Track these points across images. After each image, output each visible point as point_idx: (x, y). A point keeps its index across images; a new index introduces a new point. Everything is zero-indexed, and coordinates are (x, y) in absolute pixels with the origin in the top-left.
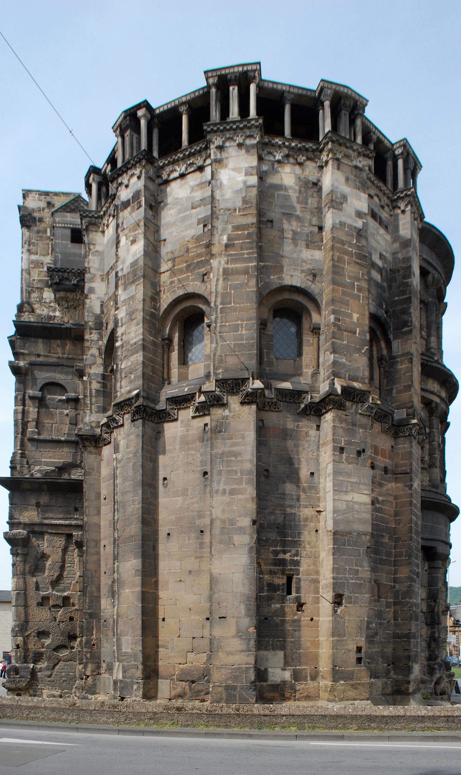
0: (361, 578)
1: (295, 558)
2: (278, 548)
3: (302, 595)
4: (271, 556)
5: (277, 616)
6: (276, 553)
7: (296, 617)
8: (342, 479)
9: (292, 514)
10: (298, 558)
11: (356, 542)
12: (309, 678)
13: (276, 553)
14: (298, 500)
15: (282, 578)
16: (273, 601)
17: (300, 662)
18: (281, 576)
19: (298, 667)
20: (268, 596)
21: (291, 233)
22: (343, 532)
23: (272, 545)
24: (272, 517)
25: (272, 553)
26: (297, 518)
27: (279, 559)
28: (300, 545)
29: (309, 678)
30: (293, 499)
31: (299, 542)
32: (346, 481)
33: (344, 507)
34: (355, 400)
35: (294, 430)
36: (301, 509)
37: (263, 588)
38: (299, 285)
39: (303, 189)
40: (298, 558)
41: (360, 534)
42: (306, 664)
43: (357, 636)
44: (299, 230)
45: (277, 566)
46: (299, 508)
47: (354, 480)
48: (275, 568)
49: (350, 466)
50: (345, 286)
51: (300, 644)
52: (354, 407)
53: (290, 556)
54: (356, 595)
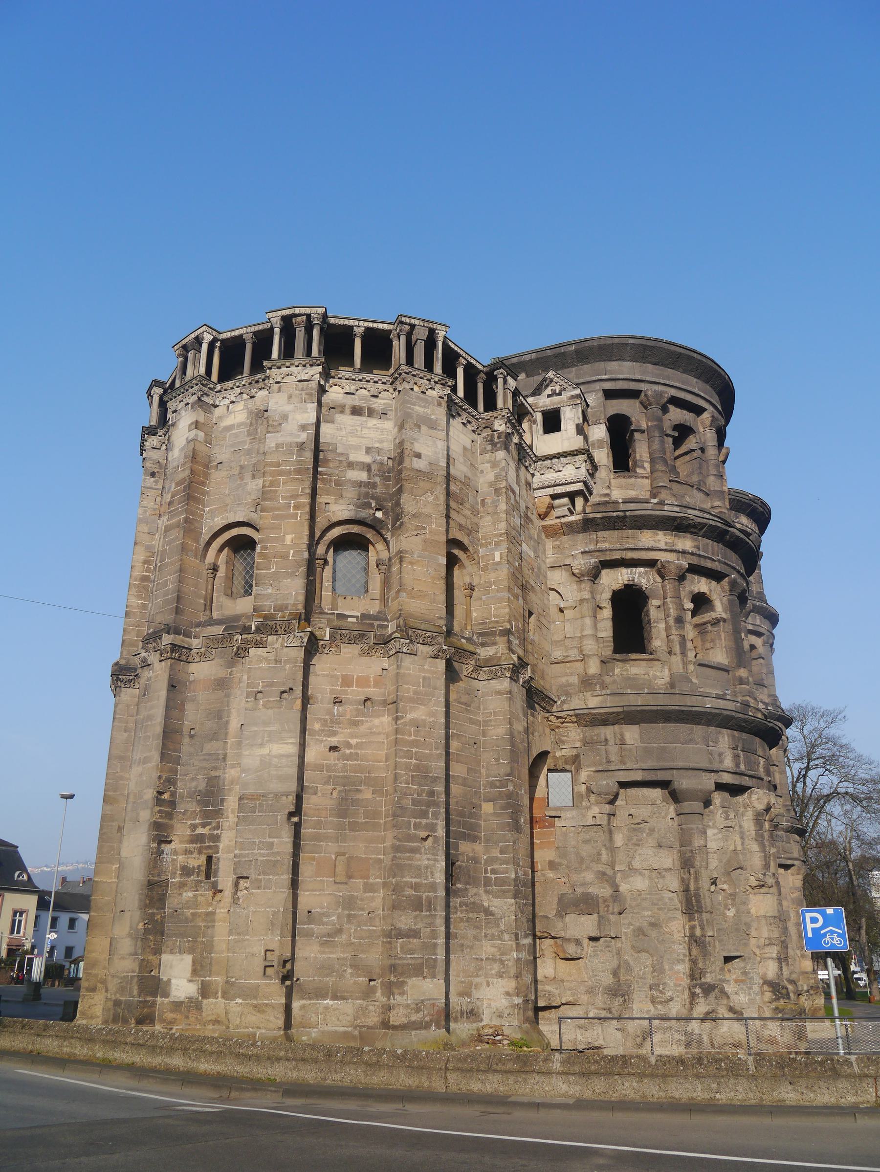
0: (277, 853)
1: (216, 832)
2: (197, 821)
3: (220, 879)
4: (188, 832)
5: (188, 908)
6: (194, 827)
7: (210, 909)
9: (216, 777)
12: (220, 994)
13: (194, 827)
14: (224, 759)
17: (210, 971)
19: (207, 978)
20: (180, 882)
21: (238, 468)
23: (190, 818)
24: (194, 784)
26: (221, 783)
27: (197, 835)
28: (222, 814)
29: (220, 994)
33: (258, 762)
38: (241, 520)
39: (254, 421)
40: (219, 832)
42: (218, 975)
43: (266, 935)
46: (224, 769)
48: (192, 846)
49: (270, 712)
52: (280, 640)
53: (210, 830)
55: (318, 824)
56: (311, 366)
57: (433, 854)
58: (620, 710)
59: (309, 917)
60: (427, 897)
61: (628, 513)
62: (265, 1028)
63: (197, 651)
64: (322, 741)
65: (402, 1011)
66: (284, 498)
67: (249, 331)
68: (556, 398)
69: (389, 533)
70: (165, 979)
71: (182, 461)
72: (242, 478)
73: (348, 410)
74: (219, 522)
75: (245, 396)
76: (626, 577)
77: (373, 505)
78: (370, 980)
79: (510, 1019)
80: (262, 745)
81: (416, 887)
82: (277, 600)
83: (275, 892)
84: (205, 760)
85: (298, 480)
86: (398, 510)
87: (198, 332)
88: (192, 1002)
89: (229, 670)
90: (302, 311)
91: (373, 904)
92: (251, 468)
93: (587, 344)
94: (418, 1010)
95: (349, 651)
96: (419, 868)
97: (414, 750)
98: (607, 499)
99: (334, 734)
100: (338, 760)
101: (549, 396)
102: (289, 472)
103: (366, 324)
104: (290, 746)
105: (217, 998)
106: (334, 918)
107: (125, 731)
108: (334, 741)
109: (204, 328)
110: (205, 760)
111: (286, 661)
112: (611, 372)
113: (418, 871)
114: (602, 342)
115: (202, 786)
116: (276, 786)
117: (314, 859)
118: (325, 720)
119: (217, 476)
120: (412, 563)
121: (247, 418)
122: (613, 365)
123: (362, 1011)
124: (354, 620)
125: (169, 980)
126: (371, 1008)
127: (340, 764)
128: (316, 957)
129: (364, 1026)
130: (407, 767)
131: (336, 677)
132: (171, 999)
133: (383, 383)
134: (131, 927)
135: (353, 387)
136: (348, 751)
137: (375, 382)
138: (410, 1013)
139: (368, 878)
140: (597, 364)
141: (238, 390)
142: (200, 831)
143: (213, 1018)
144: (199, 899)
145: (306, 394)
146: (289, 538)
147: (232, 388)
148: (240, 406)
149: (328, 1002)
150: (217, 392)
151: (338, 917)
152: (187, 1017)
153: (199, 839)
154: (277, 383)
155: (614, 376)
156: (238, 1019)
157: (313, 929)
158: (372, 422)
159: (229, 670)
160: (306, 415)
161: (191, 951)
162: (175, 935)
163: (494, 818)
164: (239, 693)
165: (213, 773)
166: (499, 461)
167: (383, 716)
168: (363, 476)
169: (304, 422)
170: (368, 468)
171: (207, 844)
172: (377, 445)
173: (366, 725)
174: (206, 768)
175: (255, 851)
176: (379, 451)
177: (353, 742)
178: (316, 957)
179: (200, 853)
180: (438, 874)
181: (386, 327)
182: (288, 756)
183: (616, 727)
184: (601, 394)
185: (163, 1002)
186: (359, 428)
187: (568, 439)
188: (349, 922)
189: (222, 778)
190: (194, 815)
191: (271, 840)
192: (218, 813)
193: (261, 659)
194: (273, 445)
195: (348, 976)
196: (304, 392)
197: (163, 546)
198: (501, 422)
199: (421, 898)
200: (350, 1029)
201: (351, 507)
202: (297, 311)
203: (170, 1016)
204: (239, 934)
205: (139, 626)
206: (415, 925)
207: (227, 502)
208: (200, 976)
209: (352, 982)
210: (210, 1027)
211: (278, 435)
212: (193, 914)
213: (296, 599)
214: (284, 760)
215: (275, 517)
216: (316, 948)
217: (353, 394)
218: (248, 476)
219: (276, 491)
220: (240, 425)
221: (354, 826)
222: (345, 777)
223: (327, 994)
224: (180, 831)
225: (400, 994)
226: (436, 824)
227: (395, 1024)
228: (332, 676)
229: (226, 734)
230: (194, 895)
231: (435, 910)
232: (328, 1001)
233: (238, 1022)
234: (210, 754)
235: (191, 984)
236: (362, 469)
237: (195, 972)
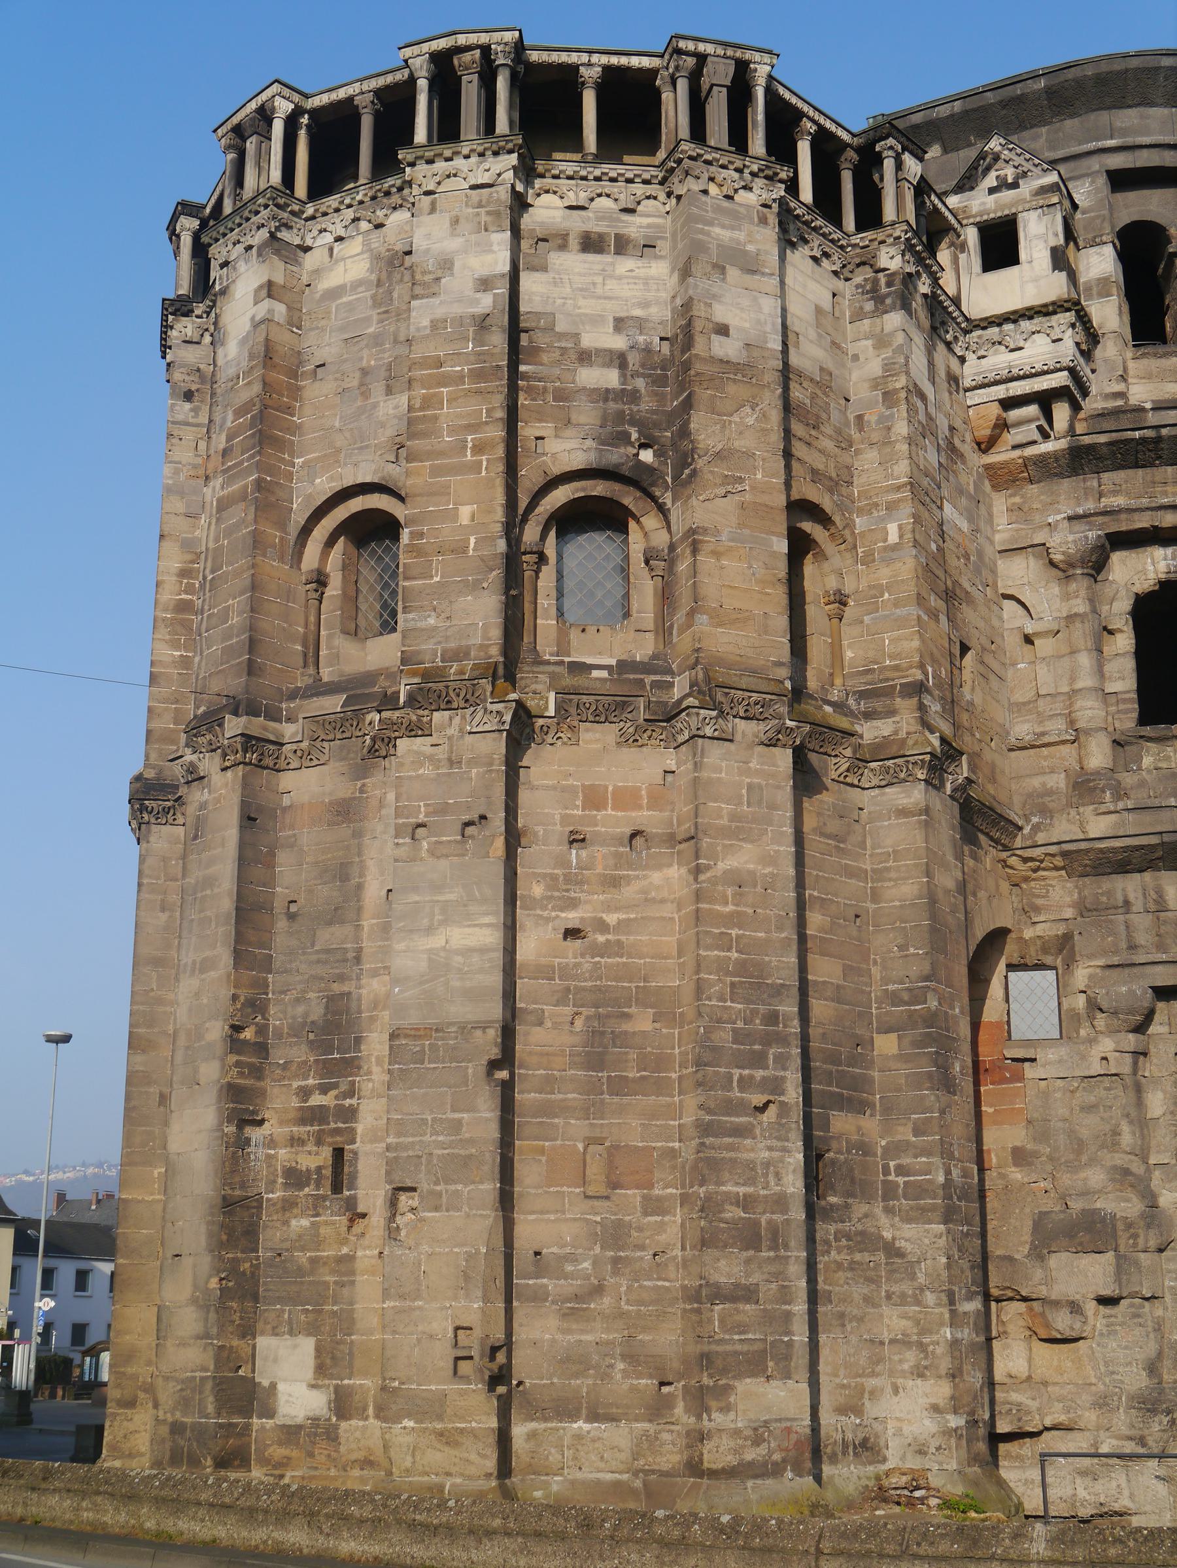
0: (471, 1142)
1: (348, 1102)
2: (311, 1082)
3: (360, 1193)
4: (295, 1103)
5: (303, 1249)
6: (305, 1093)
7: (345, 1250)
8: (417, 898)
9: (342, 995)
10: (354, 1101)
11: (454, 1048)
12: (371, 1411)
13: (305, 1093)
14: (358, 960)
15: (317, 1154)
16: (295, 1211)
17: (351, 1366)
18: (315, 1148)
19: (346, 1382)
20: (284, 1200)
21: (358, 374)
22: (418, 1029)
23: (296, 1076)
24: (300, 1009)
25: (297, 1094)
26: (354, 1005)
27: (312, 1108)
28: (359, 1068)
29: (371, 1411)
30: (346, 960)
31: (356, 1063)
32: (429, 902)
33: (424, 965)
34: (455, 705)
35: (354, 798)
36: (363, 982)
37: (275, 1182)
38: (368, 480)
39: (384, 275)
40: (354, 1101)
41: (465, 1029)
42: (365, 1374)
43: (455, 1298)
44: (373, 363)
45: (305, 1125)
46: (358, 979)
47: (451, 897)
48: (303, 1129)
49: (444, 864)
50: (441, 454)
51: (353, 1321)
52: (457, 720)
53: (337, 1097)
54: (453, 1187)
55: (549, 1084)
56: (496, 154)
57: (779, 1139)
58: (1154, 840)
59: (537, 1264)
60: (769, 1222)
61: (1164, 432)
62: (462, 1475)
63: (294, 747)
64: (548, 920)
65: (726, 1442)
66: (452, 430)
67: (365, 87)
68: (1007, 195)
69: (669, 494)
70: (266, 1383)
71: (244, 364)
72: (366, 395)
73: (574, 243)
74: (324, 486)
75: (364, 225)
76: (1162, 566)
77: (634, 436)
78: (662, 1384)
79: (940, 1458)
80: (430, 930)
81: (746, 1203)
82: (447, 638)
83: (468, 1216)
84: (318, 961)
85: (478, 392)
86: (685, 445)
87: (264, 97)
88: (318, 1426)
89: (359, 784)
90: (473, 39)
91: (663, 1238)
92: (383, 374)
93: (1070, 74)
94: (757, 1441)
95: (597, 737)
96: (750, 1166)
97: (734, 932)
98: (1120, 403)
99: (573, 904)
100: (583, 955)
101: (992, 191)
102: (460, 378)
103: (604, 60)
104: (487, 931)
105: (366, 1419)
106: (586, 1265)
107: (163, 910)
108: (572, 917)
109: (276, 88)
110: (318, 961)
111: (473, 762)
112: (1124, 132)
113: (750, 1172)
114: (1104, 67)
115: (317, 1012)
116: (460, 1011)
117: (542, 1151)
118: (554, 878)
119: (316, 392)
120: (717, 554)
121: (371, 270)
122: (1128, 118)
123: (651, 1442)
124: (604, 674)
125: (273, 1386)
126: (665, 1436)
127: (587, 964)
128: (554, 1341)
129: (653, 1472)
130: (722, 967)
131: (572, 790)
132: (279, 1420)
133: (646, 182)
134: (195, 1287)
135: (582, 195)
136: (601, 939)
137: (629, 181)
138: (743, 1447)
139: (651, 1186)
140: (1093, 116)
141: (349, 214)
142: (317, 1100)
143: (359, 1455)
144: (322, 1231)
145: (488, 213)
146: (465, 512)
147: (337, 210)
148: (355, 246)
149: (581, 1425)
150: (307, 220)
151: (594, 1264)
152: (311, 1455)
153: (316, 1116)
154: (428, 193)
155: (1129, 141)
156: (409, 1459)
157: (546, 1286)
158: (626, 265)
159: (359, 784)
160: (489, 258)
161: (312, 1329)
162: (279, 1300)
163: (899, 1065)
164: (380, 828)
165: (337, 988)
166: (892, 334)
167: (670, 865)
168: (611, 378)
169: (485, 272)
170: (619, 360)
171: (333, 1125)
172: (638, 312)
173: (636, 886)
174: (322, 978)
175: (427, 1138)
176: (641, 324)
177: (611, 919)
178: (554, 1341)
179: (319, 1142)
180: (791, 1177)
181: (645, 62)
182: (482, 950)
183: (1147, 876)
184: (1102, 180)
186: (599, 279)
187: (1036, 280)
188: (616, 1272)
189: (354, 996)
191: (457, 1116)
192: (351, 1066)
193: (420, 759)
194: (426, 322)
195: (619, 1376)
196: (483, 210)
197: (217, 540)
198: (893, 251)
199: (757, 1223)
200: (625, 1477)
201: (589, 443)
202: (462, 40)
203: (278, 1452)
204: (402, 1297)
205: (177, 702)
206: (747, 1276)
207: (338, 444)
208: (331, 1377)
209: (625, 1387)
210: (356, 1472)
211: (435, 301)
212: (313, 1261)
213: (485, 637)
214: (475, 958)
215: (436, 471)
216: (553, 1322)
217: (583, 208)
218: (378, 389)
219: (436, 418)
220: (357, 284)
221: (619, 1086)
222: (598, 989)
223: (578, 1410)
224: (280, 1102)
225: (721, 1410)
226: (783, 1079)
227: (714, 1467)
228: (564, 789)
229: (359, 910)
230: (313, 1223)
231: (786, 1247)
232: (580, 1423)
233: (408, 1463)
234: (328, 951)
236: (608, 365)
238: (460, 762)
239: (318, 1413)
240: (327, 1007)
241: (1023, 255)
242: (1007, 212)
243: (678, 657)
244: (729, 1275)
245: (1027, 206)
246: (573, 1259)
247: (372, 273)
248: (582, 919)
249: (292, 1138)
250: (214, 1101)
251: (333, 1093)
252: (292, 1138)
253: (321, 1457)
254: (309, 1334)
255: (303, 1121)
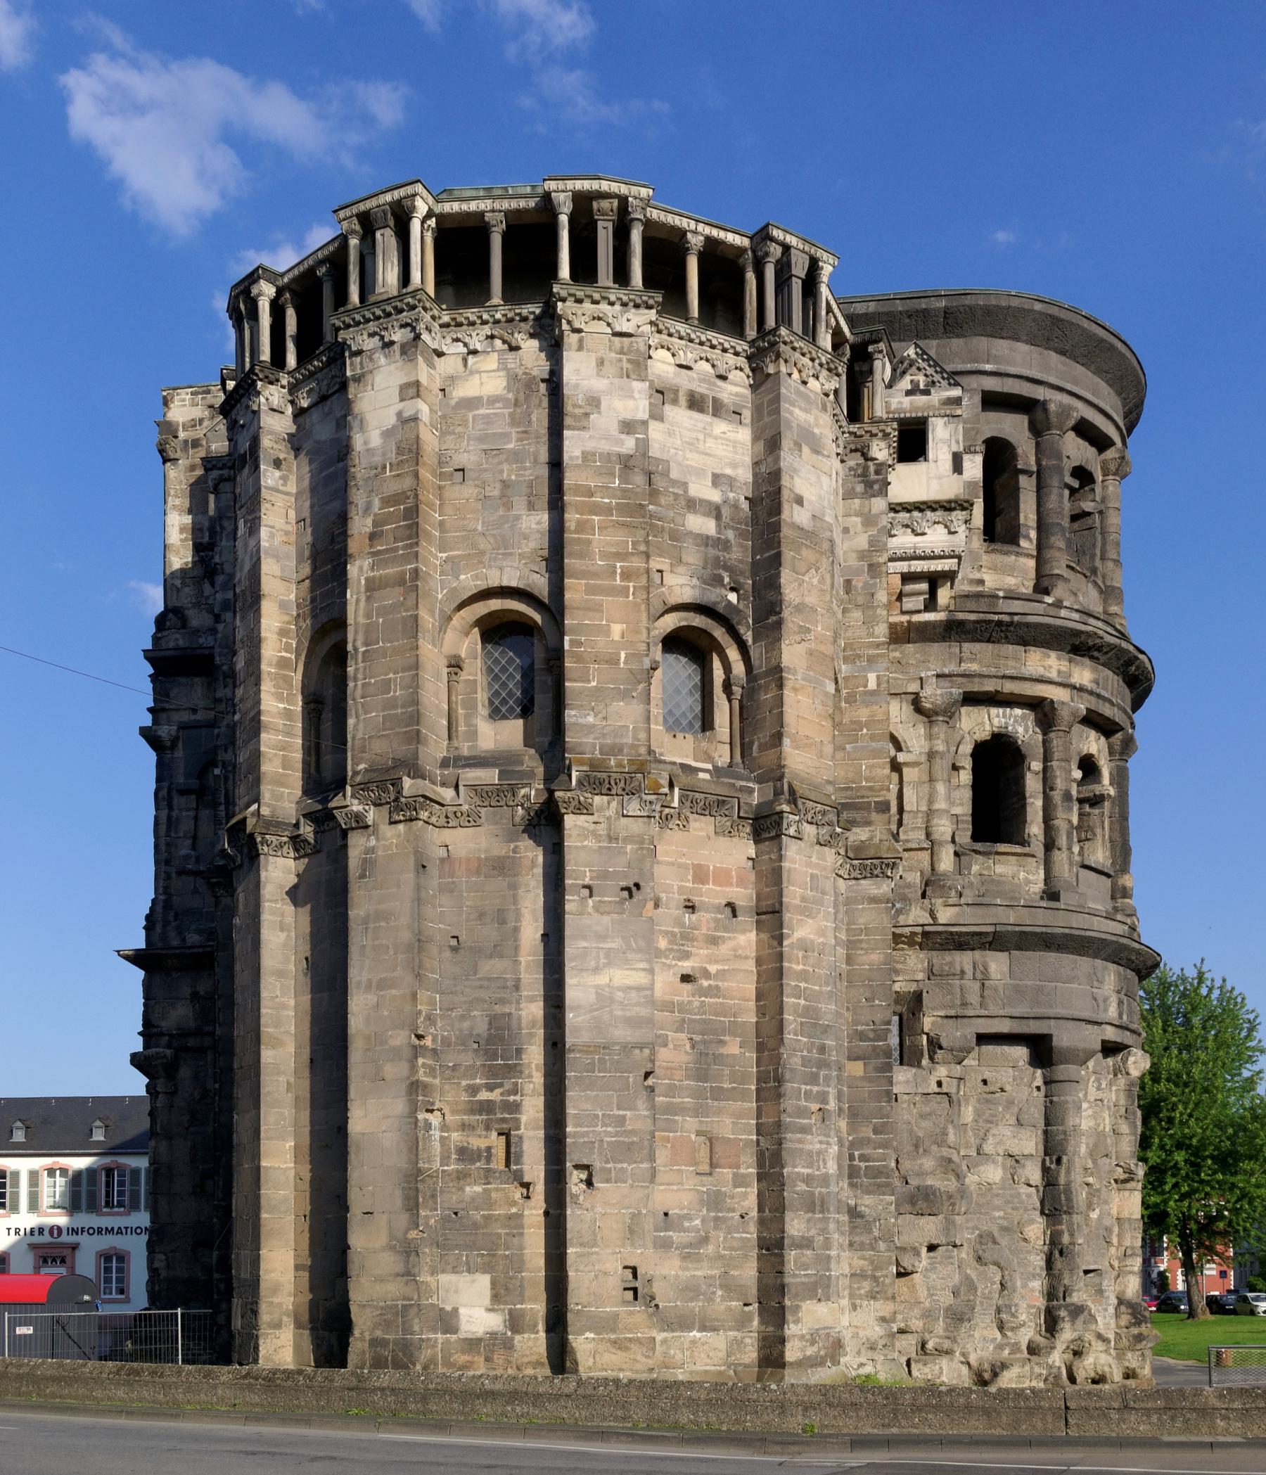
1: (512, 1098)
3: (526, 1168)
4: (464, 1097)
6: (474, 1090)
7: (514, 1210)
9: (503, 1015)
10: (518, 1098)
13: (474, 1090)
14: (517, 987)
17: (522, 1295)
19: (518, 1306)
23: (464, 1077)
24: (466, 1024)
25: (466, 1090)
26: (514, 1024)
27: (480, 1102)
28: (521, 1072)
36: (522, 1005)
37: (449, 1157)
39: (522, 397)
40: (518, 1098)
46: (518, 1003)
48: (472, 1117)
53: (502, 1094)
55: (672, 1090)
57: (825, 1135)
59: (665, 1222)
64: (670, 966)
68: (920, 400)
69: (750, 633)
70: (448, 1308)
77: (727, 580)
82: (604, 736)
85: (624, 525)
95: (702, 826)
96: (810, 1153)
97: (803, 985)
99: (686, 956)
100: (693, 995)
101: (908, 393)
102: (608, 510)
105: (537, 1332)
108: (686, 966)
115: (482, 1028)
117: (668, 1139)
118: (673, 935)
120: (795, 690)
121: (508, 388)
123: (737, 1344)
124: (706, 776)
125: (456, 1310)
127: (696, 1002)
131: (683, 867)
132: (462, 1335)
142: (484, 1095)
144: (494, 1195)
148: (491, 362)
149: (695, 1334)
153: (486, 1107)
162: (457, 1247)
163: (864, 1084)
165: (498, 1009)
166: (878, 516)
168: (708, 526)
173: (730, 944)
179: (488, 1128)
184: (978, 399)
185: (448, 1340)
187: (940, 478)
189: (515, 1016)
190: (470, 1071)
192: (513, 1070)
199: (813, 1194)
201: (695, 581)
204: (582, 1245)
206: (809, 1230)
208: (506, 1303)
212: (486, 1218)
216: (677, 1262)
219: (589, 542)
223: (694, 1323)
228: (680, 866)
231: (828, 1211)
232: (694, 1333)
235: (492, 1315)
237: (496, 1298)
238: (617, 839)
239: (495, 1329)
240: (490, 1024)
241: (931, 454)
242: (920, 414)
243: (760, 768)
244: (799, 1231)
245: (937, 413)
246: (688, 1217)
247: (509, 391)
248: (693, 968)
249: (463, 1125)
250: (403, 1093)
251: (498, 1091)
252: (463, 1125)
253: (499, 1358)
254: (485, 1272)
255: (472, 1112)
